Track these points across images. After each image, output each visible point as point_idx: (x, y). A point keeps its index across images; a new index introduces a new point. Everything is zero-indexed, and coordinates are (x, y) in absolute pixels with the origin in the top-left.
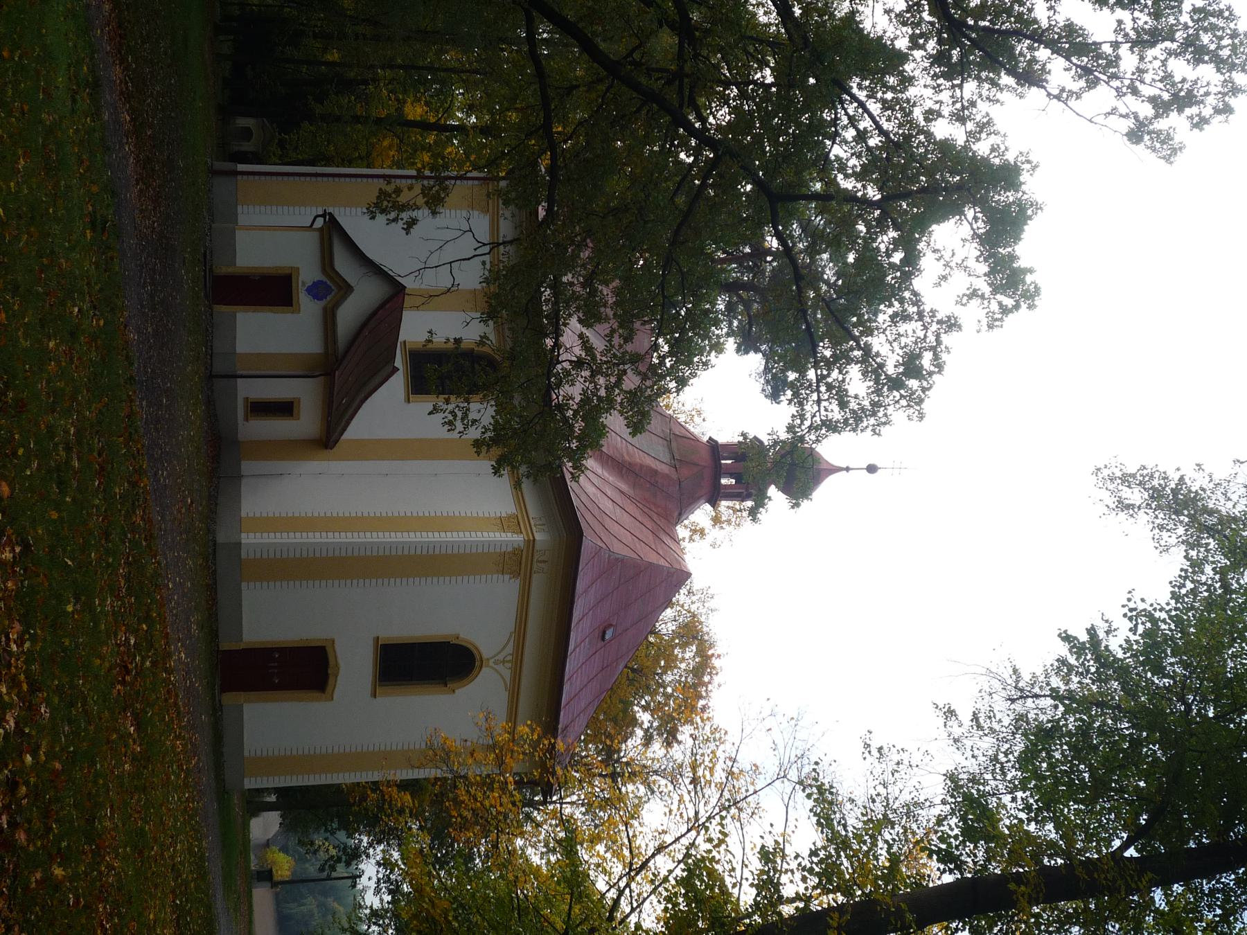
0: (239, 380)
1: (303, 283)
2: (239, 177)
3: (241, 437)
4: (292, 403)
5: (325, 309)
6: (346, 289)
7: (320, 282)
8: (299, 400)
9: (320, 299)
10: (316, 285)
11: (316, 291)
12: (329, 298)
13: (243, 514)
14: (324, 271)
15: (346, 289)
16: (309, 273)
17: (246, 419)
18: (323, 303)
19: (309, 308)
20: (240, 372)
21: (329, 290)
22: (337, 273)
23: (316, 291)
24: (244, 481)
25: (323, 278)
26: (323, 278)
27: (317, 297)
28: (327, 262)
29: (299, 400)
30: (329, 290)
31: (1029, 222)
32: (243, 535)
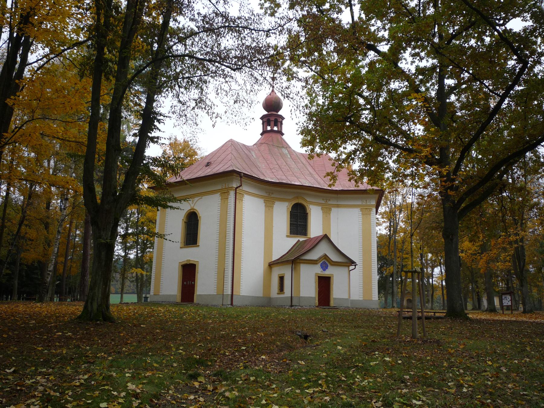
2: (234, 294)
5: (332, 265)
6: (325, 257)
7: (321, 265)
10: (322, 268)
11: (324, 267)
12: (327, 263)
13: (362, 299)
14: (317, 264)
15: (325, 257)
16: (317, 270)
19: (330, 271)
23: (324, 267)
25: (319, 265)
26: (319, 265)
27: (327, 268)
28: (313, 262)
30: (324, 263)
32: (373, 299)
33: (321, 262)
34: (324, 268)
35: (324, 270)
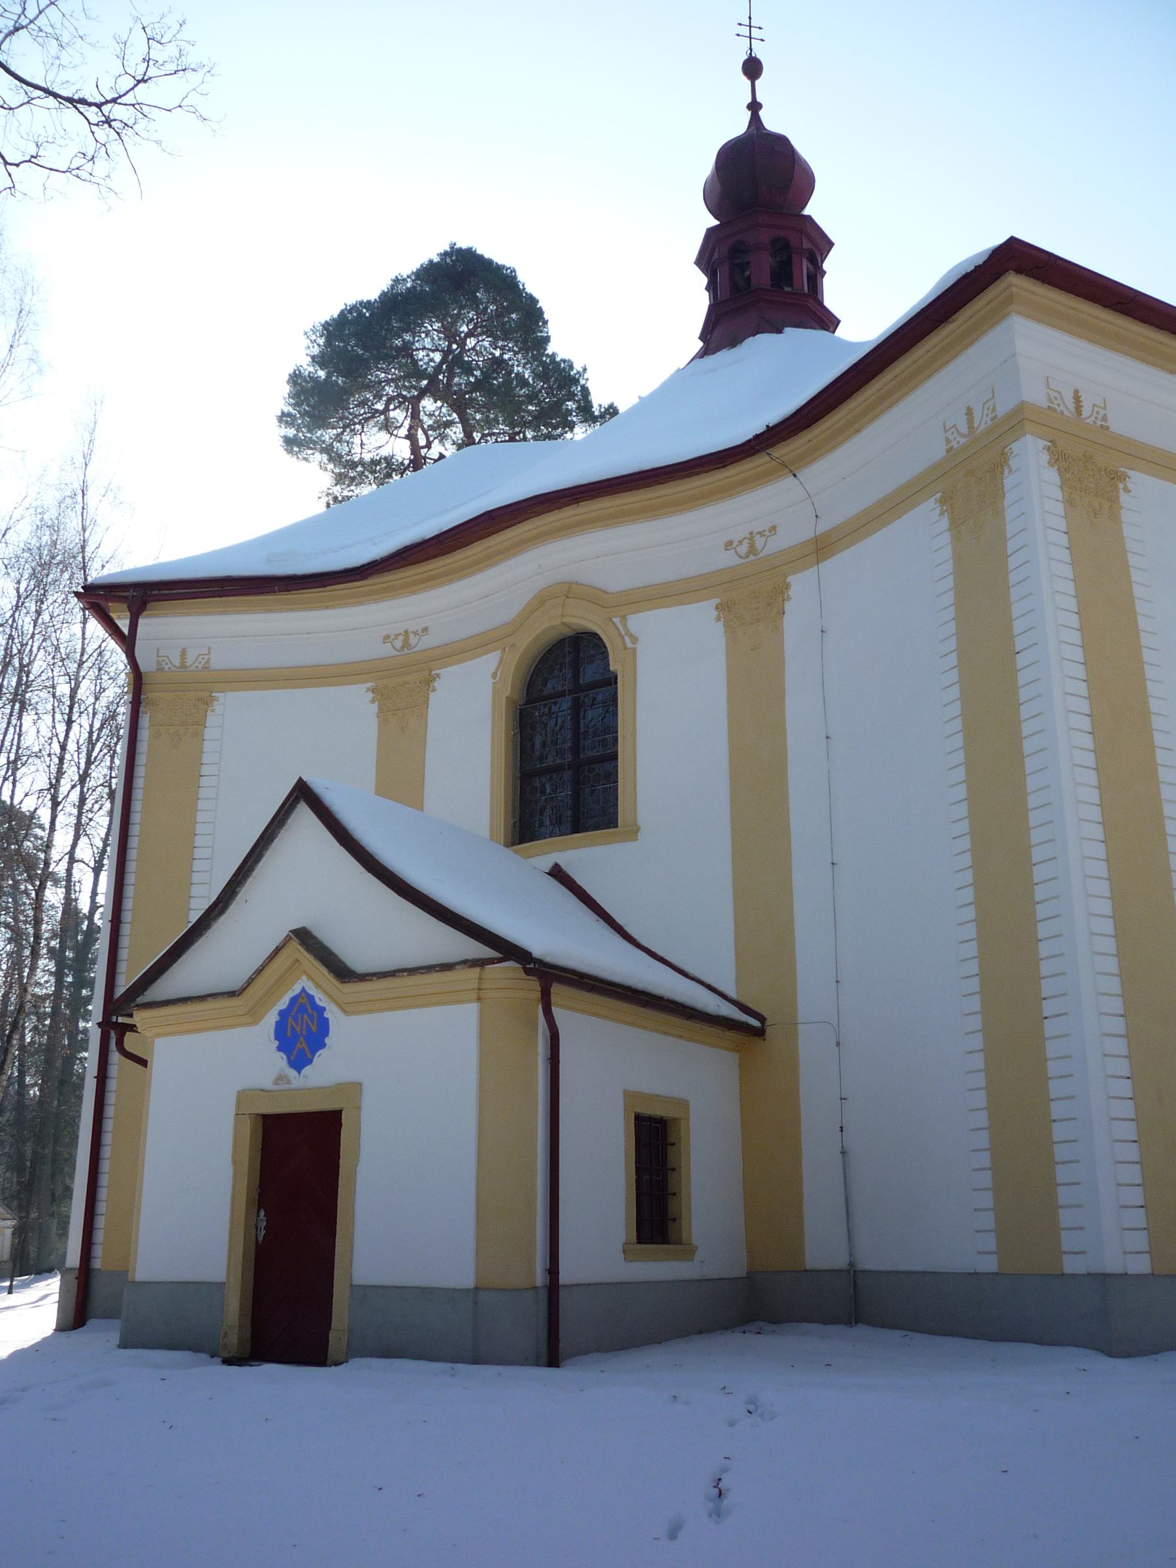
0: (564, 1278)
1: (280, 1078)
3: (735, 1267)
4: (639, 1119)
8: (629, 1096)
9: (324, 1027)
12: (321, 1000)
17: (689, 1252)
18: (332, 1013)
20: (540, 1278)
21: (304, 1006)
22: (251, 981)
24: (867, 1262)
26: (272, 1018)
29: (629, 1096)
31: (415, 270)
33: (283, 1003)
34: (302, 1044)
35: (299, 1062)
